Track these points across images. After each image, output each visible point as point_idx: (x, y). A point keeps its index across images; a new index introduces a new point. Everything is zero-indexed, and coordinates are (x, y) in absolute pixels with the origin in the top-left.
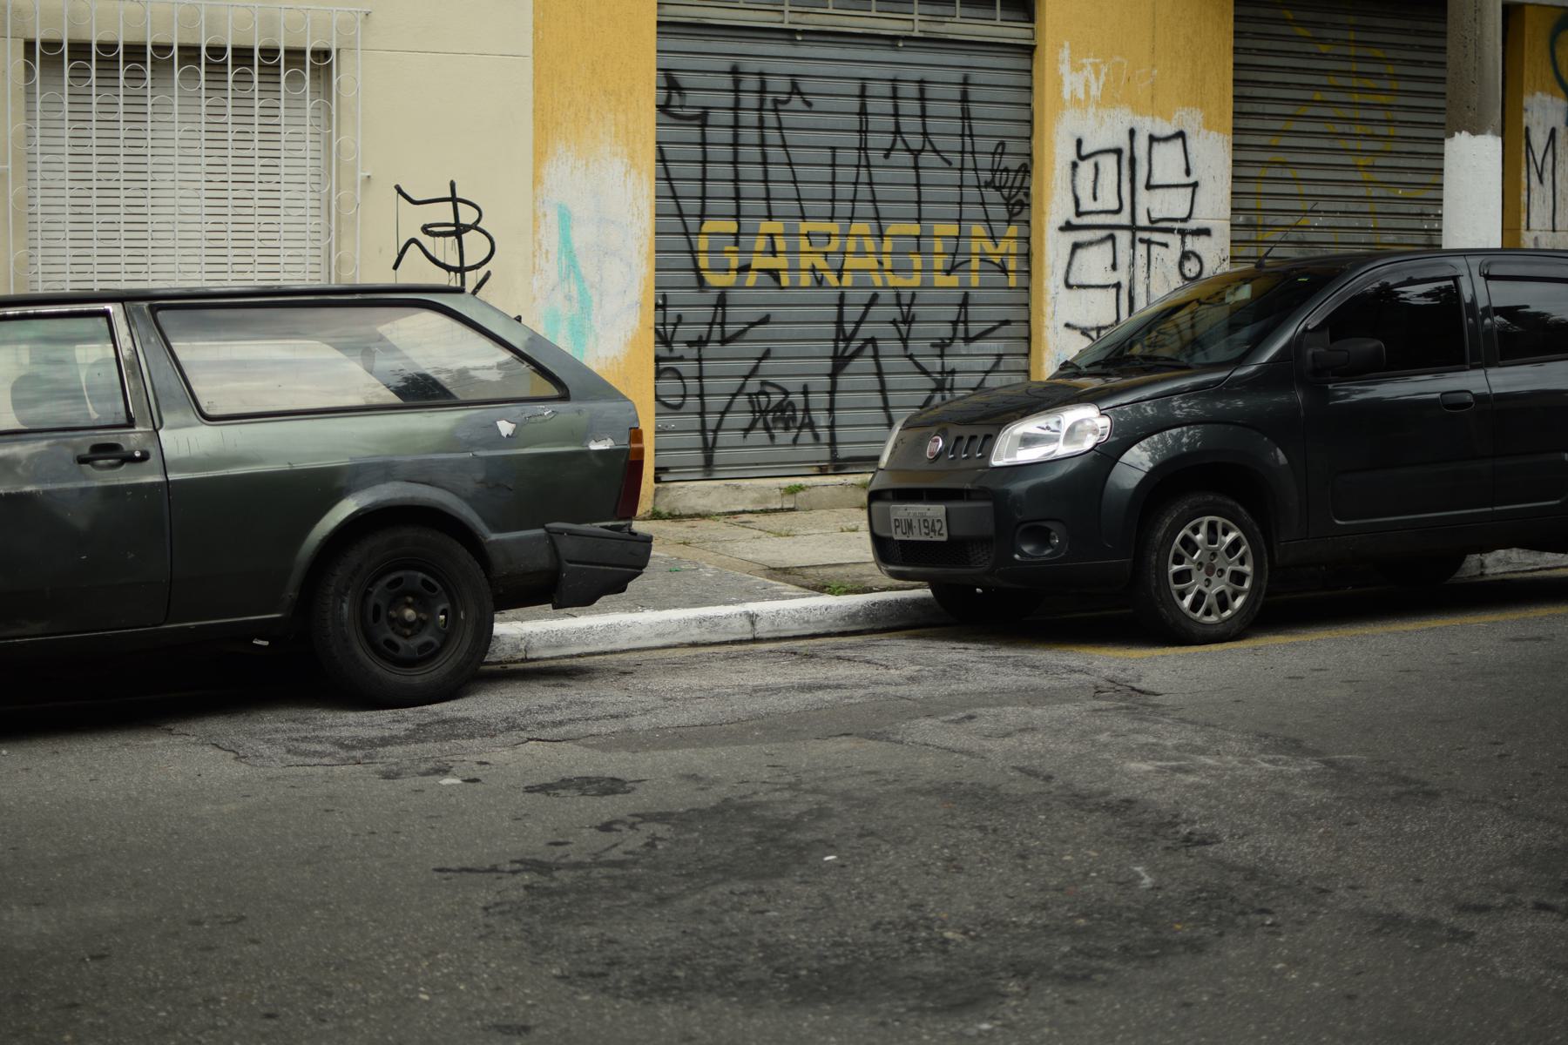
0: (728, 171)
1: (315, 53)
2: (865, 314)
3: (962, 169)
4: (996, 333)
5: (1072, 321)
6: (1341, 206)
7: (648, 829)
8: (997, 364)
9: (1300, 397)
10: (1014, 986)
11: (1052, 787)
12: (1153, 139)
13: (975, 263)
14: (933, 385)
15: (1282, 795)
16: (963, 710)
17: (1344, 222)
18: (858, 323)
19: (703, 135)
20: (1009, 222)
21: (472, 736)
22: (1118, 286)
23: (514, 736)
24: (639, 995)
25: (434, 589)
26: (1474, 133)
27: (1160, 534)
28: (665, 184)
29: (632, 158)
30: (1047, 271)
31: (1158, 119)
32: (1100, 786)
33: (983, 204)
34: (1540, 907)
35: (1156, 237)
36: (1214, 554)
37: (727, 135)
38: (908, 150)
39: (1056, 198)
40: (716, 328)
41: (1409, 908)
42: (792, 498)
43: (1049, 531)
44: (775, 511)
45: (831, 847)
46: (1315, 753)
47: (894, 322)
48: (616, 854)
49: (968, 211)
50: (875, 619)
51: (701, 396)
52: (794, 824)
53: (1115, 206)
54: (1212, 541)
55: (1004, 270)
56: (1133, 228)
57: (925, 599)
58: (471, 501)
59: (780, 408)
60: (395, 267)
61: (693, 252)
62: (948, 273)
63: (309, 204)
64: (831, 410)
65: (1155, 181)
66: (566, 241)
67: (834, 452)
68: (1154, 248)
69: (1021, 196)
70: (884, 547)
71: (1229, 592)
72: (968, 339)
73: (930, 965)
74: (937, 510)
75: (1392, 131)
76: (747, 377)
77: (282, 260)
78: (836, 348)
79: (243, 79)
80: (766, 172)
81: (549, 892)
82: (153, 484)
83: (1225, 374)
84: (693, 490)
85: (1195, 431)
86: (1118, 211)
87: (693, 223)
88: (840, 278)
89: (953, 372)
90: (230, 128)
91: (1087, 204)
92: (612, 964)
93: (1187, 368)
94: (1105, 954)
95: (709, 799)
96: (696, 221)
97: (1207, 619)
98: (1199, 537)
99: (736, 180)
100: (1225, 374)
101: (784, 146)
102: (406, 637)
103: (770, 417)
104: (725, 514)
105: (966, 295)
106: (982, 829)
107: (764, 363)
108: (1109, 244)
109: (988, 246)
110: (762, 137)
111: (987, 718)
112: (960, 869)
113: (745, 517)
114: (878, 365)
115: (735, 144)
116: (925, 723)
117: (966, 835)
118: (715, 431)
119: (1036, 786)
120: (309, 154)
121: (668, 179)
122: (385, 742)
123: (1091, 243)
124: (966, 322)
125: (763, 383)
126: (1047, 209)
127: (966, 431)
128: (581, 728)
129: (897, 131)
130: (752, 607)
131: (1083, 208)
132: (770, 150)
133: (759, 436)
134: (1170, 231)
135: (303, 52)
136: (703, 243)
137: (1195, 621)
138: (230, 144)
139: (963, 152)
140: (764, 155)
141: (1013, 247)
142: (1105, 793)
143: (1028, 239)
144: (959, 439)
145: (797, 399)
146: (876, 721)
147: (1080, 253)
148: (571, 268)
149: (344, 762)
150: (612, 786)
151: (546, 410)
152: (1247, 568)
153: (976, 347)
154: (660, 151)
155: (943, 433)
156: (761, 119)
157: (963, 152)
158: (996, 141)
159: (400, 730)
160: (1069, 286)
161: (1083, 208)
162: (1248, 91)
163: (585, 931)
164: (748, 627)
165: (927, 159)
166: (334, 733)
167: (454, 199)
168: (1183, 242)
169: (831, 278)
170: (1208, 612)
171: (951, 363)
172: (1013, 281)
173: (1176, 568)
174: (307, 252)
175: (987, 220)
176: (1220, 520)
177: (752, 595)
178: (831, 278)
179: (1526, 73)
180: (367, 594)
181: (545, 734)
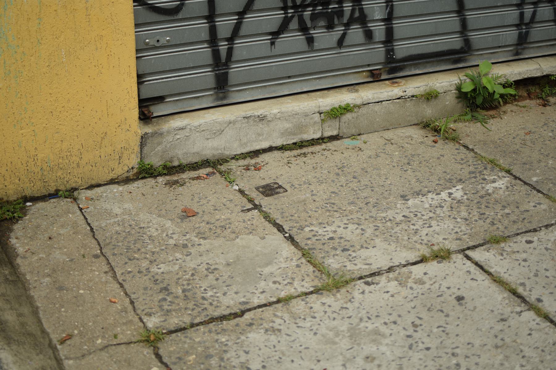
42: (336, 123)
67: (390, 52)
84: (199, 129)
103: (307, 13)
104: (244, 156)
133: (293, 39)
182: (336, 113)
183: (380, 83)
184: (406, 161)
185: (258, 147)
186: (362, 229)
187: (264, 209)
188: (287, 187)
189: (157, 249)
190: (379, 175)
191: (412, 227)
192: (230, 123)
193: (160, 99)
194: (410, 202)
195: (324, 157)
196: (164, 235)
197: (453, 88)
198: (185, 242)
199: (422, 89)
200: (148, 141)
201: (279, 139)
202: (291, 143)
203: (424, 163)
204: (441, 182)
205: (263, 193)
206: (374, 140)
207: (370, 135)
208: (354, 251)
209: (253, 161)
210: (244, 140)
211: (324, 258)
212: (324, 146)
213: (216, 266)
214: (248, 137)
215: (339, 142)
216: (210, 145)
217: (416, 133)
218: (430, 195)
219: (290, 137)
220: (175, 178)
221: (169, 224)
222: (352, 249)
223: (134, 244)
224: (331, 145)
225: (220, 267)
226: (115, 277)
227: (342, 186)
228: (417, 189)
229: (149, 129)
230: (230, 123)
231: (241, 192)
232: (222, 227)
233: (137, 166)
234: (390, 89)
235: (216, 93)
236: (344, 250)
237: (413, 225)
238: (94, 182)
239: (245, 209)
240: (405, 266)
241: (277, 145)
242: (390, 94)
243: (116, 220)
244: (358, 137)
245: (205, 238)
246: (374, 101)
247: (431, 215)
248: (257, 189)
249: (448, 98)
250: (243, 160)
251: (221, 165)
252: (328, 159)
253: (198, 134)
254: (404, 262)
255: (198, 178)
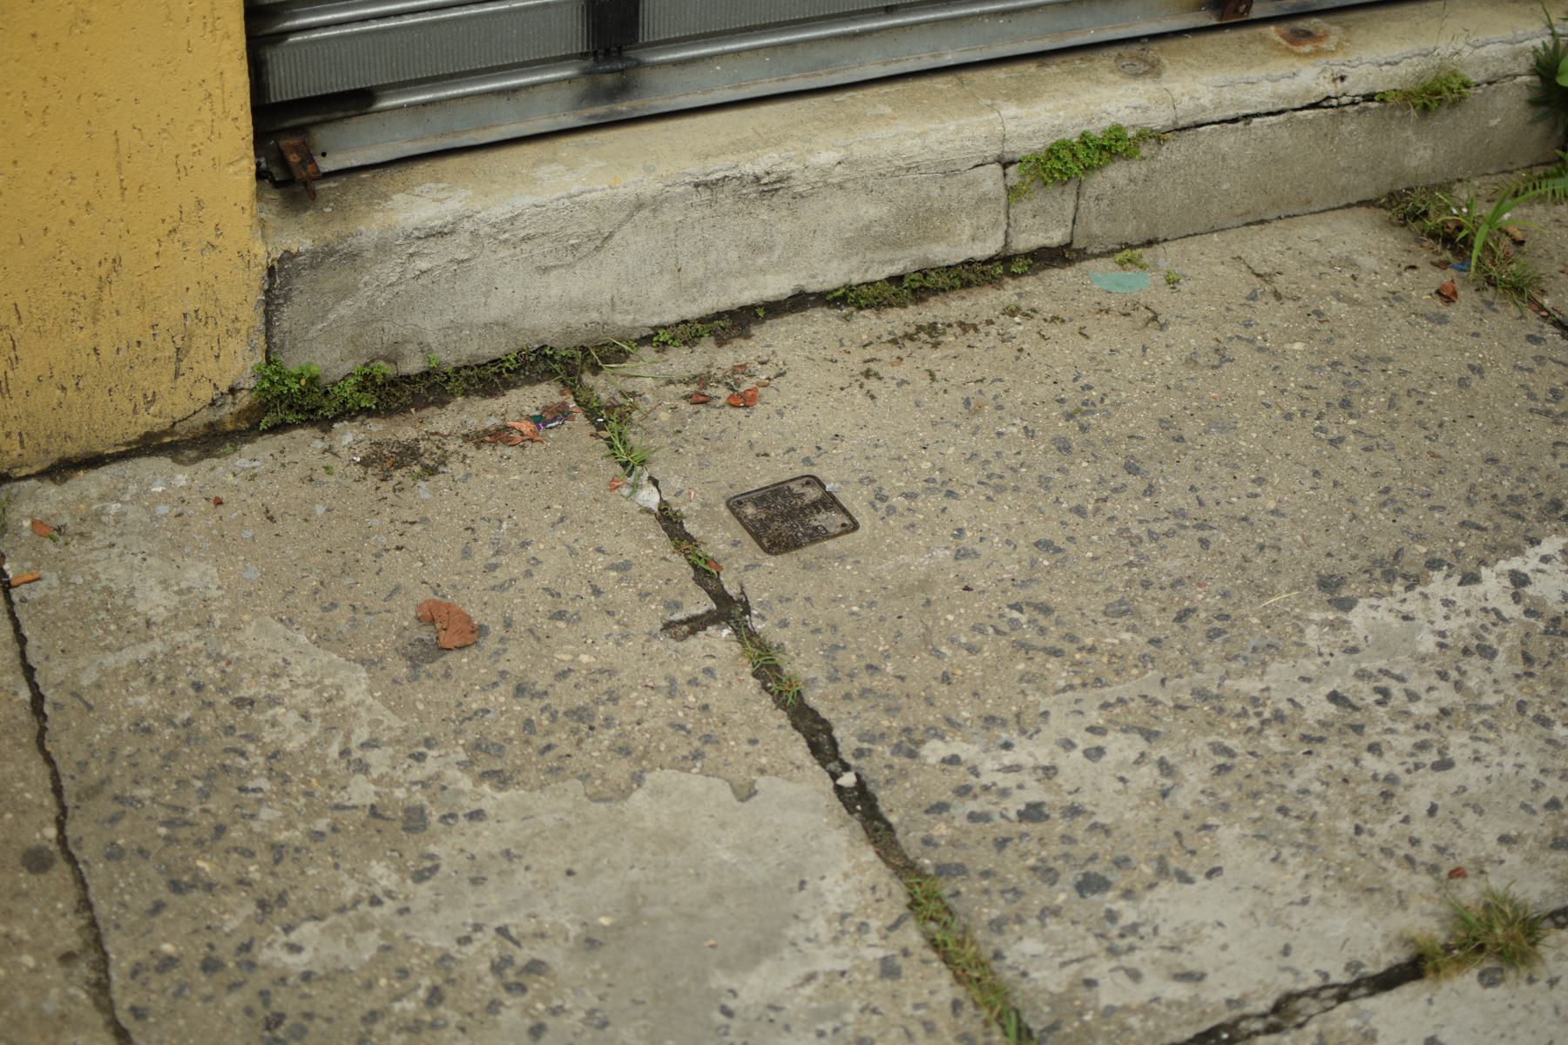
84: (507, 233)
104: (688, 332)
182: (1064, 164)
183: (1246, 33)
184: (1335, 391)
185: (748, 297)
186: (1164, 767)
187: (758, 626)
188: (855, 500)
189: (293, 836)
190: (1229, 459)
191: (1369, 760)
192: (640, 206)
193: (359, 101)
194: (1358, 618)
195: (1007, 351)
196: (334, 750)
197: (1524, 64)
198: (419, 797)
199: (1404, 70)
200: (298, 284)
201: (835, 264)
202: (883, 276)
203: (1407, 404)
204: (1481, 513)
205: (757, 531)
206: (1209, 266)
207: (1193, 245)
208: (1128, 894)
209: (725, 358)
210: (695, 269)
211: (997, 926)
212: (1008, 293)
213: (538, 951)
214: (712, 257)
215: (1068, 273)
216: (555, 291)
217: (1368, 245)
218: (1440, 585)
219: (878, 256)
220: (405, 431)
221: (357, 686)
222: (1120, 879)
223: (205, 795)
224: (1037, 289)
225: (553, 955)
226: (101, 987)
227: (1079, 511)
228: (1383, 547)
229: (299, 237)
230: (640, 206)
231: (669, 520)
232: (579, 714)
233: (252, 383)
234: (1281, 66)
235: (586, 73)
236: (1090, 885)
237: (1374, 748)
238: (72, 450)
239: (678, 616)
240: (1343, 994)
241: (827, 287)
242: (1284, 87)
243: (143, 652)
244: (1146, 255)
245: (501, 779)
246: (1217, 116)
247: (1446, 695)
248: (735, 505)
249: (1499, 102)
250: (685, 350)
251: (596, 370)
252: (1025, 359)
253: (504, 253)
254: (1340, 976)
255: (500, 435)
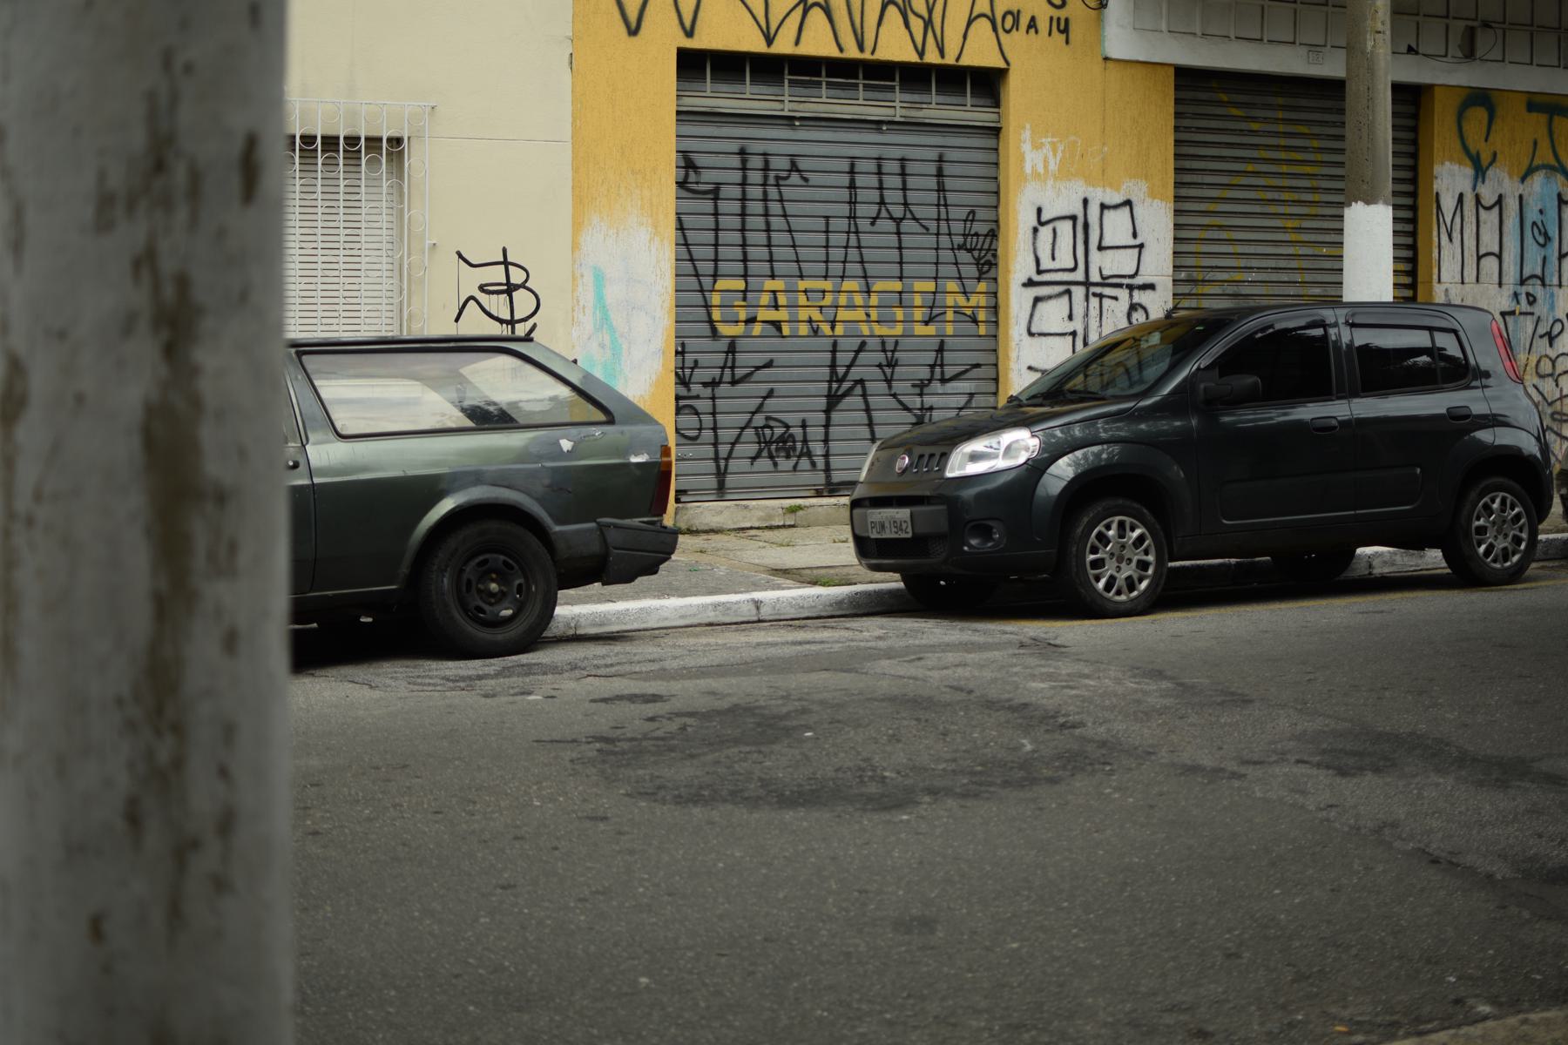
0: (736, 237)
1: (390, 140)
2: (855, 359)
3: (938, 234)
4: (968, 375)
5: (1034, 364)
6: (1272, 263)
7: (679, 721)
8: (969, 401)
9: (1194, 422)
10: (927, 799)
11: (972, 697)
12: (1103, 207)
13: (950, 315)
14: (914, 420)
15: (1139, 702)
16: (916, 655)
17: (1274, 277)
18: (849, 367)
19: (716, 207)
20: (979, 279)
21: (545, 673)
22: (1074, 334)
23: (577, 673)
24: (678, 803)
25: (512, 568)
26: (1368, 202)
27: (1079, 530)
28: (683, 249)
29: (656, 227)
30: (1012, 321)
31: (1108, 190)
32: (1007, 696)
33: (956, 264)
34: (1298, 762)
35: (1107, 291)
36: (1123, 547)
37: (736, 207)
38: (891, 218)
39: (1020, 259)
40: (728, 372)
41: (1207, 762)
43: (991, 528)
44: (778, 527)
45: (809, 728)
46: (1171, 678)
47: (880, 366)
48: (659, 733)
49: (943, 270)
50: (858, 605)
51: (715, 429)
52: (787, 716)
53: (1072, 265)
54: (1122, 536)
55: (975, 321)
56: (1087, 284)
57: (898, 590)
58: (539, 500)
59: (783, 439)
60: (457, 320)
61: (707, 306)
62: (926, 323)
63: (385, 267)
64: (826, 441)
65: (1105, 243)
66: (600, 298)
67: (828, 477)
68: (1106, 302)
69: (989, 257)
70: (866, 547)
71: (1135, 577)
72: (943, 381)
73: (873, 789)
74: (903, 513)
75: (1317, 197)
76: (753, 413)
77: (363, 314)
78: (830, 388)
79: (331, 163)
80: (769, 238)
81: (613, 753)
82: (302, 487)
83: (1131, 404)
85: (1116, 448)
86: (1074, 269)
87: (707, 281)
88: (833, 328)
89: (931, 408)
90: (319, 203)
91: (1046, 263)
92: (659, 788)
93: (1103, 399)
94: (991, 784)
95: (725, 704)
96: (710, 280)
97: (1118, 598)
98: (1111, 533)
99: (744, 245)
100: (1131, 404)
101: (785, 216)
102: (491, 604)
103: (773, 447)
105: (942, 342)
106: (918, 720)
107: (768, 401)
108: (1066, 298)
109: (961, 300)
110: (766, 208)
111: (932, 659)
112: (899, 741)
113: (753, 532)
114: (866, 403)
115: (743, 214)
116: (885, 663)
117: (905, 723)
118: (727, 459)
119: (963, 696)
120: (385, 225)
121: (686, 244)
122: (480, 678)
123: (1050, 297)
124: (942, 365)
125: (767, 418)
126: (1012, 268)
127: (927, 450)
128: (627, 668)
129: (882, 202)
130: (757, 595)
131: (1043, 267)
132: (772, 219)
134: (1120, 286)
135: (380, 140)
136: (716, 299)
137: (1109, 600)
138: (319, 217)
139: (938, 220)
140: (768, 224)
141: (983, 300)
142: (1009, 700)
143: (995, 294)
144: (921, 456)
145: (797, 432)
146: (849, 662)
147: (1040, 305)
148: (604, 321)
149: (452, 689)
150: (655, 698)
151: (597, 431)
152: (1151, 558)
153: (951, 386)
154: (679, 220)
155: (909, 453)
156: (765, 193)
157: (938, 220)
158: (968, 210)
159: (491, 670)
160: (1031, 334)
161: (1043, 267)
162: (1188, 164)
163: (641, 772)
164: (754, 611)
165: (907, 225)
166: (442, 673)
167: (506, 263)
168: (1131, 296)
169: (825, 328)
170: (1119, 593)
171: (929, 400)
172: (982, 330)
173: (1092, 557)
174: (384, 307)
175: (960, 278)
176: (1128, 520)
177: (757, 587)
178: (825, 328)
179: (1436, 145)
180: (462, 571)
181: (599, 672)
182: (793, 510)
